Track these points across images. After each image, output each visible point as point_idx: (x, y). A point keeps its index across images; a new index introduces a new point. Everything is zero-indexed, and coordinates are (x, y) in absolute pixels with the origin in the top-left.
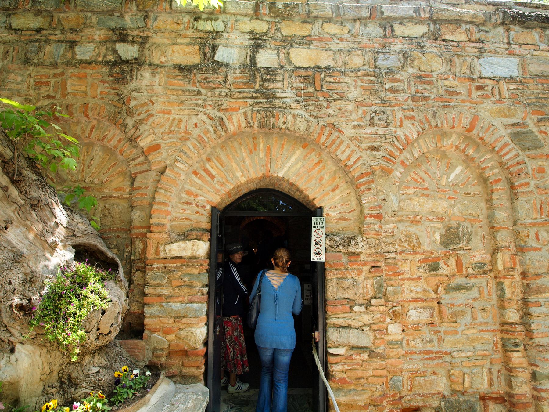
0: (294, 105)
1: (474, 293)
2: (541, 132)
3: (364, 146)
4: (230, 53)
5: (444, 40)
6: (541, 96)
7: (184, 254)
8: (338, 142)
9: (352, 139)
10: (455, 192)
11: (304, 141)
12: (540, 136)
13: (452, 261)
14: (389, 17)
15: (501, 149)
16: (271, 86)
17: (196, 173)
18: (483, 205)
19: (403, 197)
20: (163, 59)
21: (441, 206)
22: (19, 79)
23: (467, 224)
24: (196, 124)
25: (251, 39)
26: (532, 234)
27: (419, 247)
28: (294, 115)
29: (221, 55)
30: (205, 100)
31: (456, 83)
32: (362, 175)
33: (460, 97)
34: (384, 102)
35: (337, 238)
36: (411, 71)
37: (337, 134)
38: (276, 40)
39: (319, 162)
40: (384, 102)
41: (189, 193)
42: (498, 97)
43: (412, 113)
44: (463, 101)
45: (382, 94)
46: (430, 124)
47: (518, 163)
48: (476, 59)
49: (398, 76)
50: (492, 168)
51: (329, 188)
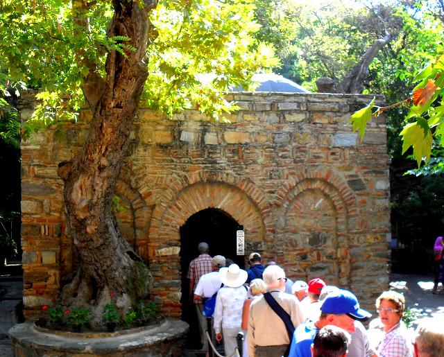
0: (226, 168)
1: (326, 271)
2: (365, 180)
3: (266, 190)
4: (189, 136)
5: (314, 123)
6: (368, 157)
7: (168, 254)
8: (252, 189)
9: (259, 187)
10: (319, 214)
11: (233, 188)
12: (364, 182)
13: (315, 253)
14: (282, 110)
15: (342, 191)
16: (214, 156)
17: (170, 207)
18: (333, 221)
19: (288, 218)
20: (150, 141)
21: (310, 222)
22: (65, 153)
23: (324, 232)
24: (171, 180)
25: (201, 125)
26: (356, 238)
27: (296, 247)
28: (227, 174)
29: (184, 136)
30: (176, 165)
31: (320, 151)
32: (265, 208)
33: (321, 160)
34: (278, 164)
35: (251, 243)
36: (294, 144)
37: (251, 184)
38: (215, 126)
39: (241, 199)
40: (278, 164)
41: (167, 219)
42: (343, 159)
43: (293, 171)
44: (323, 162)
45: (277, 159)
46: (303, 176)
47: (351, 198)
48: (332, 136)
49: (286, 148)
50: (338, 201)
51: (246, 215)
